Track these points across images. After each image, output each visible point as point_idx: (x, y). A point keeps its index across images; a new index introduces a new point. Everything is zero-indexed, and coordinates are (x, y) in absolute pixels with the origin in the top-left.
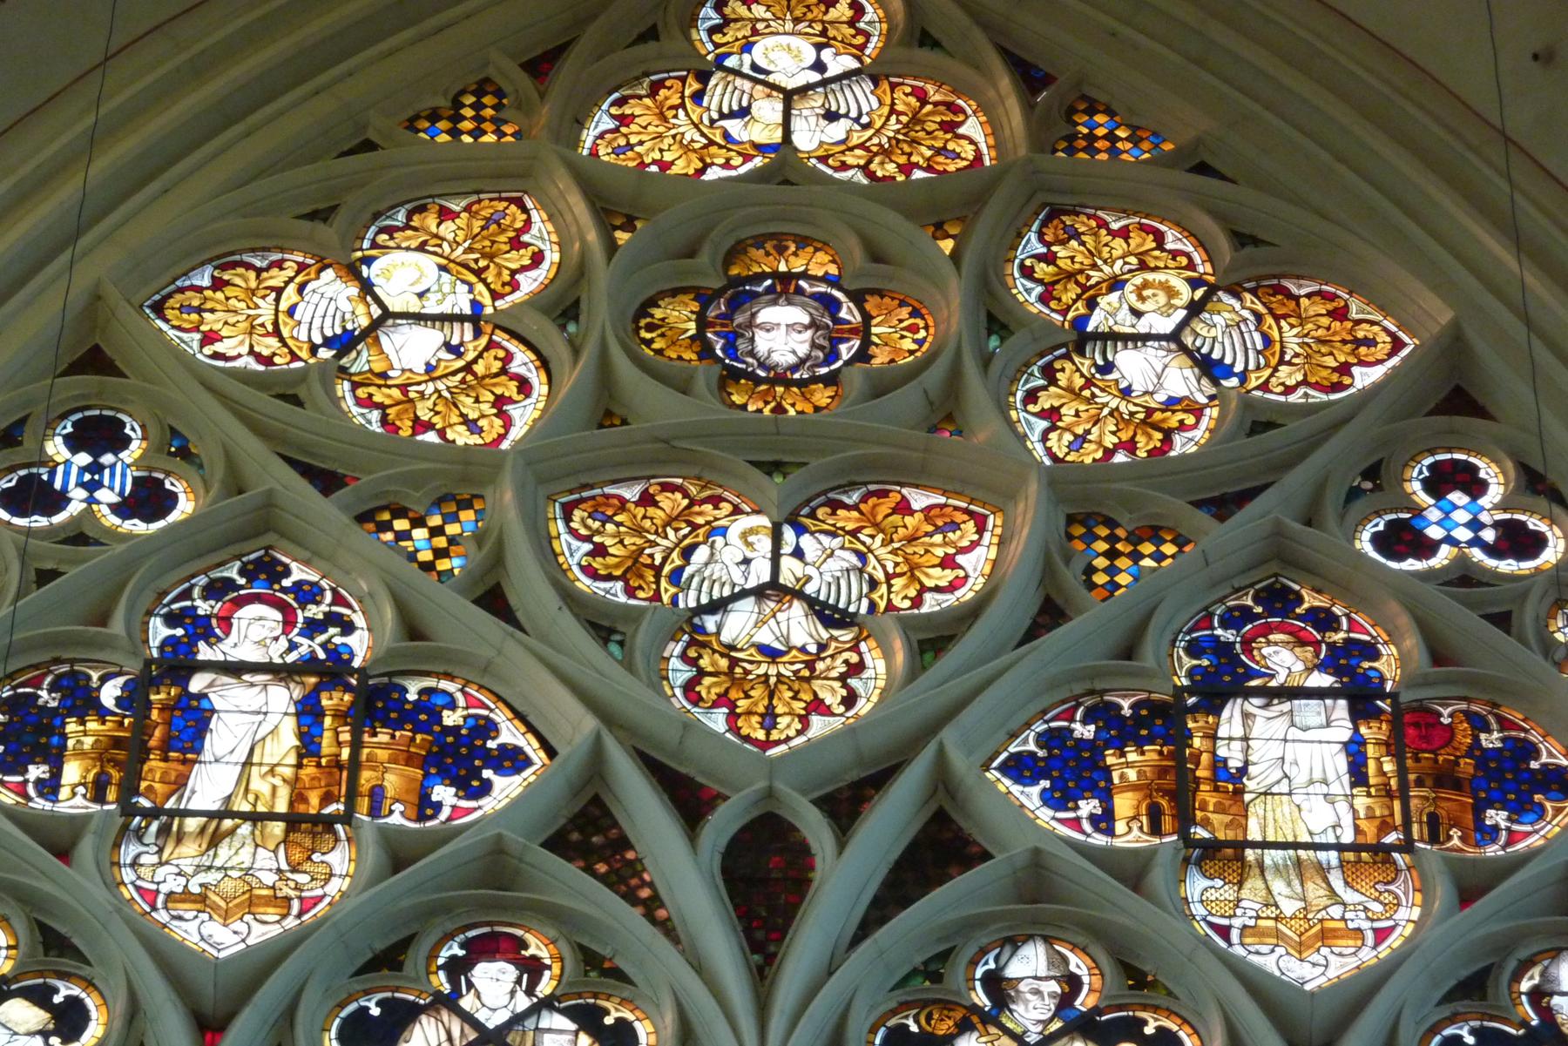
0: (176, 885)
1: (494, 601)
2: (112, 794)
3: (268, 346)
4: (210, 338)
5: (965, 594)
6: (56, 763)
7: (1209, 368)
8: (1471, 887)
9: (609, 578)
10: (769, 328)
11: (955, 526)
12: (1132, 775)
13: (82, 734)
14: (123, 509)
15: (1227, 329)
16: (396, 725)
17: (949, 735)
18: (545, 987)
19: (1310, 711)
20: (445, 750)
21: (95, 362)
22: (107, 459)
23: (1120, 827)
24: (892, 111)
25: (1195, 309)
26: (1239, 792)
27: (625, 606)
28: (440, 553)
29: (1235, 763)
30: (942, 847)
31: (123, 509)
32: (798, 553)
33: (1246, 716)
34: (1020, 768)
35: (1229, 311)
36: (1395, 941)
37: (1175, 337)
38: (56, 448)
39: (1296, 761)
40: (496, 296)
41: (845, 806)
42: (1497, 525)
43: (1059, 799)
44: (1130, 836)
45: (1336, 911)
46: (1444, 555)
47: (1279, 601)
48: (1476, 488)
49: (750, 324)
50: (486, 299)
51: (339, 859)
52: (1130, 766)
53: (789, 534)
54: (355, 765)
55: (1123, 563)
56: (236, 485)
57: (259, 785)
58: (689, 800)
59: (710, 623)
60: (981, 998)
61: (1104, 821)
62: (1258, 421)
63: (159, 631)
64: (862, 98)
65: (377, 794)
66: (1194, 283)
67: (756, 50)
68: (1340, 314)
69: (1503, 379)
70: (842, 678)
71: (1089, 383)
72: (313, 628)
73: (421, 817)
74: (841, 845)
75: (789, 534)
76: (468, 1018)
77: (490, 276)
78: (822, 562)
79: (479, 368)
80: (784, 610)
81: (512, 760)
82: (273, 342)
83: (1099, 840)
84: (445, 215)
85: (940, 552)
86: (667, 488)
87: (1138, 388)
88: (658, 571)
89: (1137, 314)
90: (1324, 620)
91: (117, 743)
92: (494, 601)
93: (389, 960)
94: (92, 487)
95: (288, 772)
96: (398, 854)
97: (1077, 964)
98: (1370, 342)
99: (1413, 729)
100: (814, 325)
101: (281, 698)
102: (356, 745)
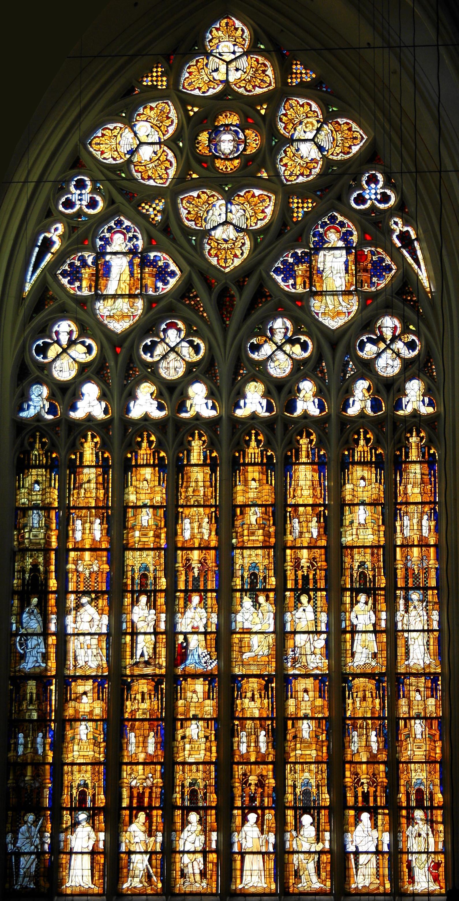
0: (107, 314)
2: (93, 290)
3: (116, 154)
4: (102, 153)
5: (266, 221)
6: (80, 280)
7: (321, 149)
9: (191, 221)
10: (224, 141)
11: (264, 200)
12: (300, 272)
13: (86, 273)
14: (88, 206)
16: (149, 266)
17: (262, 267)
18: (183, 335)
19: (337, 253)
20: (160, 272)
22: (83, 192)
23: (298, 287)
24: (251, 67)
25: (318, 130)
26: (322, 277)
27: (195, 229)
28: (156, 215)
29: (321, 269)
31: (88, 206)
32: (231, 212)
33: (325, 255)
34: (277, 271)
36: (352, 315)
37: (313, 140)
38: (72, 189)
40: (164, 135)
42: (381, 193)
45: (340, 308)
46: (369, 202)
47: (333, 219)
48: (376, 182)
49: (220, 141)
50: (162, 137)
52: (301, 269)
53: (229, 206)
54: (142, 279)
55: (300, 210)
57: (122, 286)
59: (213, 233)
60: (269, 334)
61: (294, 285)
64: (243, 62)
65: (146, 286)
66: (318, 121)
67: (220, 47)
68: (350, 129)
70: (241, 247)
71: (294, 155)
72: (131, 239)
73: (156, 292)
74: (241, 295)
75: (229, 206)
76: (167, 344)
77: (162, 128)
78: (237, 214)
79: (161, 159)
81: (173, 274)
82: (116, 153)
83: (293, 291)
84: (152, 109)
85: (261, 208)
86: (203, 193)
87: (305, 156)
88: (202, 217)
89: (305, 132)
91: (93, 275)
94: (80, 200)
95: (128, 282)
98: (356, 138)
99: (359, 258)
100: (234, 140)
101: (124, 261)
102: (141, 273)
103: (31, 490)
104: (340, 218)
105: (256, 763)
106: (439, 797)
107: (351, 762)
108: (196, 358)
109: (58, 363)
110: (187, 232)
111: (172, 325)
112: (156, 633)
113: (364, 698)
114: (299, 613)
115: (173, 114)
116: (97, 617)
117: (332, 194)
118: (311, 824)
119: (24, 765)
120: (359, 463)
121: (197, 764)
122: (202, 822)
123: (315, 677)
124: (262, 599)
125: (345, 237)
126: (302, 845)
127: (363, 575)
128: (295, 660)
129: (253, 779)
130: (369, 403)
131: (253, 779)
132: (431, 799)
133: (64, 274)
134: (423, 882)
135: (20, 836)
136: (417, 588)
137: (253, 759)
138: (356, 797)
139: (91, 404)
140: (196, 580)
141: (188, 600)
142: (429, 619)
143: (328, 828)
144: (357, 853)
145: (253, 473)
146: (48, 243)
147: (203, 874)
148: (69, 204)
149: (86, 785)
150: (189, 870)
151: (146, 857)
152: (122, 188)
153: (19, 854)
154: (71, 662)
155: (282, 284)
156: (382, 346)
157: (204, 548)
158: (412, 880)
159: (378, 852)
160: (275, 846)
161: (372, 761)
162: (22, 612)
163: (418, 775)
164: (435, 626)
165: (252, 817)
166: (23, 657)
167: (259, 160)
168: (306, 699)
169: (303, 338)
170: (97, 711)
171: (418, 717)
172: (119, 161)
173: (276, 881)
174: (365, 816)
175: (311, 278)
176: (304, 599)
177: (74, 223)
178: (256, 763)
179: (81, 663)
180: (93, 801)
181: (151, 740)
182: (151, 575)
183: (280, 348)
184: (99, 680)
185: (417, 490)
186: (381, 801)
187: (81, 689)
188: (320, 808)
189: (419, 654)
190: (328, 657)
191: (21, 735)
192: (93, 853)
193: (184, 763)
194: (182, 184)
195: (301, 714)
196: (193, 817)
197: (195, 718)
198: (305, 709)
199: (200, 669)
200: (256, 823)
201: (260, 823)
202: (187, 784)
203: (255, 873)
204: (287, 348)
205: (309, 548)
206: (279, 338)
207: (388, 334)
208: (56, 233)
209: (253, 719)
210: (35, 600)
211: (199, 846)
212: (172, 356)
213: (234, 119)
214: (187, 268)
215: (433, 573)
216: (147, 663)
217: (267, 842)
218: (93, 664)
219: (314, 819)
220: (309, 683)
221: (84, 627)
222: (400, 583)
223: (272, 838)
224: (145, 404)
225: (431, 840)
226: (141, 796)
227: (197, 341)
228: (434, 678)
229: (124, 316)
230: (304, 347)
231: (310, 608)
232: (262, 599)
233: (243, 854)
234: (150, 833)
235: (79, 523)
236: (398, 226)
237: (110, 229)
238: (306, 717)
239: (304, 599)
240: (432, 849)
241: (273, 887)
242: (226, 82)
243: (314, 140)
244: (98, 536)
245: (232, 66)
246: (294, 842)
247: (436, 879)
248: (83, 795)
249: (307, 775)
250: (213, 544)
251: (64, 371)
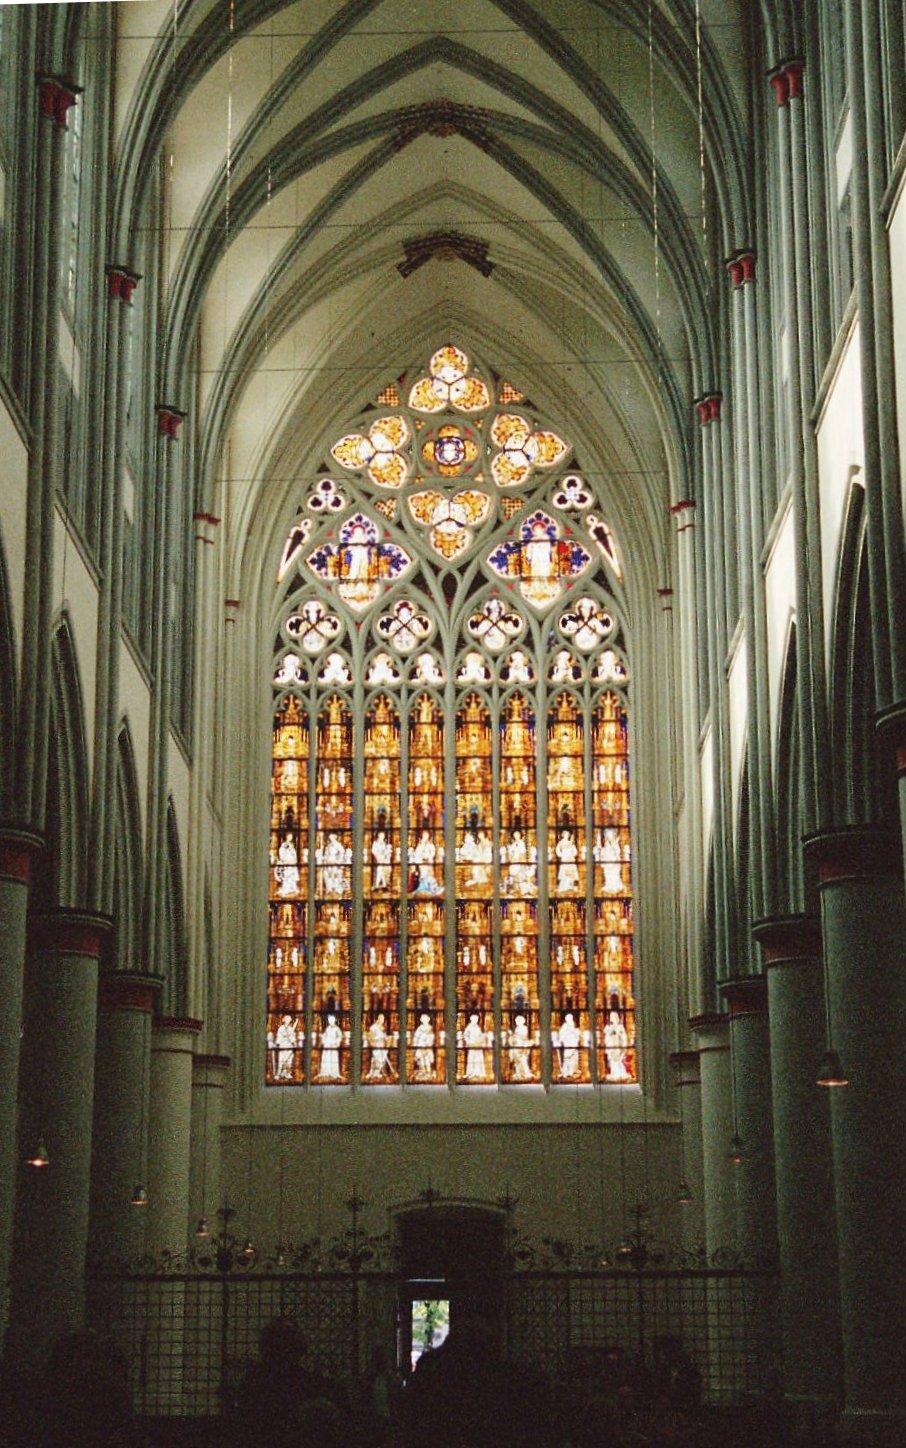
1: (400, 525)
7: (528, 457)
8: (570, 584)
13: (330, 561)
15: (532, 447)
21: (324, 469)
30: (480, 580)
34: (493, 560)
35: (533, 440)
39: (540, 556)
41: (462, 570)
43: (500, 567)
44: (512, 576)
47: (539, 516)
51: (377, 588)
56: (353, 501)
58: (436, 570)
62: (537, 472)
63: (342, 536)
64: (463, 385)
69: (582, 462)
80: (452, 522)
81: (405, 562)
90: (547, 521)
92: (400, 525)
93: (386, 609)
96: (388, 587)
97: (502, 605)
99: (561, 547)
103: (286, 745)
104: (545, 516)
105: (478, 973)
106: (630, 1001)
107: (557, 973)
108: (423, 633)
109: (307, 637)
110: (419, 529)
111: (405, 605)
112: (392, 865)
113: (567, 919)
114: (512, 848)
115: (404, 428)
116: (341, 849)
117: (537, 495)
119: (282, 975)
120: (563, 722)
121: (428, 974)
122: (432, 1023)
123: (527, 901)
124: (481, 835)
125: (549, 531)
127: (566, 816)
128: (510, 887)
129: (475, 987)
130: (571, 671)
131: (475, 987)
132: (624, 1003)
133: (313, 561)
134: (618, 1071)
135: (279, 1034)
136: (612, 826)
137: (474, 970)
138: (561, 1001)
139: (336, 671)
140: (426, 820)
141: (418, 837)
142: (622, 853)
144: (562, 1049)
145: (473, 729)
146: (299, 536)
147: (434, 1066)
148: (316, 503)
149: (334, 992)
150: (421, 1063)
151: (386, 1052)
152: (364, 491)
153: (278, 1050)
154: (321, 889)
155: (497, 571)
156: (581, 623)
157: (433, 793)
158: (608, 1071)
159: (580, 1048)
161: (575, 971)
162: (279, 846)
163: (613, 983)
164: (627, 858)
165: (474, 1019)
166: (280, 884)
167: (476, 465)
168: (519, 920)
169: (514, 617)
170: (344, 930)
171: (613, 934)
172: (359, 467)
174: (569, 1018)
175: (520, 566)
176: (517, 835)
177: (321, 518)
178: (478, 973)
179: (329, 889)
180: (341, 1005)
181: (389, 954)
182: (388, 816)
183: (495, 624)
184: (346, 904)
185: (612, 744)
186: (583, 1004)
187: (329, 911)
188: (530, 1012)
189: (613, 882)
190: (536, 883)
191: (279, 951)
192: (341, 1049)
193: (416, 974)
194: (412, 487)
195: (515, 932)
196: (425, 1019)
197: (426, 935)
198: (519, 928)
199: (429, 894)
201: (481, 1024)
202: (419, 990)
204: (501, 624)
205: (521, 793)
206: (494, 616)
207: (586, 614)
208: (307, 527)
209: (474, 936)
210: (290, 837)
211: (430, 1044)
212: (404, 630)
213: (455, 433)
214: (417, 558)
215: (625, 814)
216: (385, 890)
218: (340, 891)
220: (521, 906)
221: (332, 859)
222: (597, 822)
224: (381, 673)
225: (624, 1037)
226: (380, 1002)
227: (425, 619)
228: (626, 901)
229: (364, 598)
230: (516, 624)
231: (521, 843)
232: (481, 835)
234: (389, 1032)
235: (327, 771)
236: (593, 522)
237: (351, 524)
238: (519, 935)
239: (517, 835)
240: (625, 1044)
241: (492, 1076)
242: (449, 401)
243: (524, 451)
244: (343, 782)
245: (453, 388)
247: (628, 1070)
248: (331, 1001)
249: (520, 983)
250: (440, 789)
251: (313, 644)
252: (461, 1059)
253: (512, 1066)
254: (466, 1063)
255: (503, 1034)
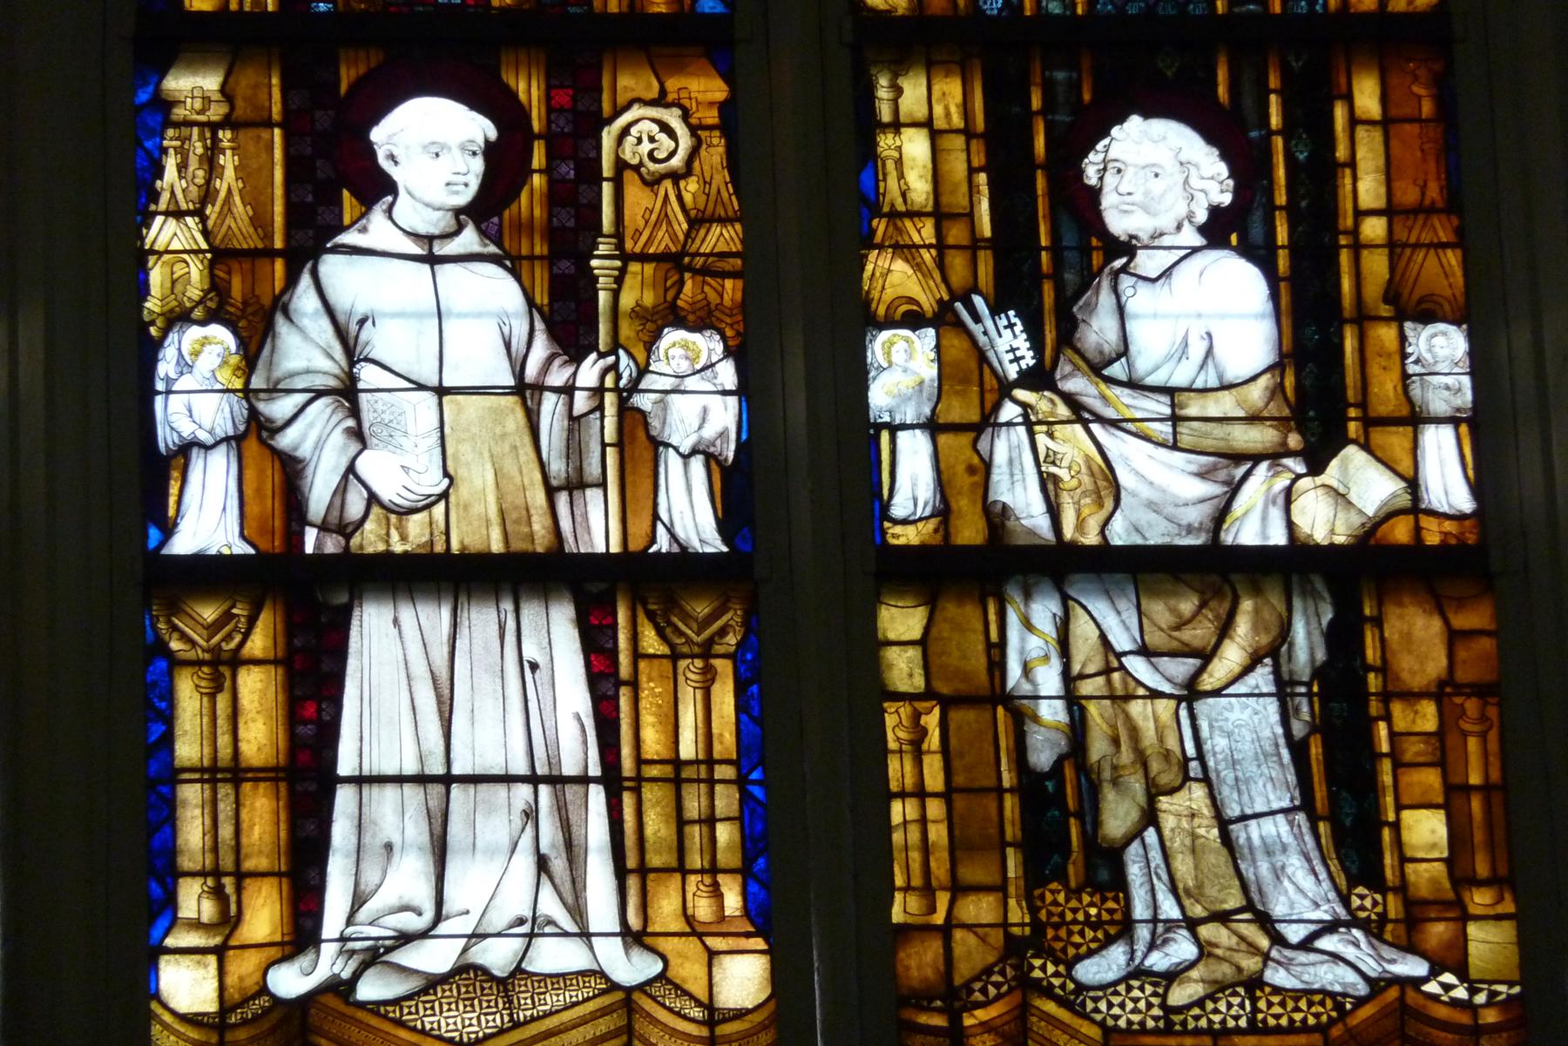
118: (1219, 229)
126: (1107, 485)
143: (1443, 270)
160: (737, 484)
165: (432, 144)
173: (762, 918)
200: (484, 209)
201: (540, 217)
203: (487, 822)
217: (639, 442)
219: (1247, 166)
223: (696, 393)
233: (309, 589)
246: (1008, 447)
252: (227, 715)
253: (1057, 829)
254: (308, 776)
255: (901, 369)
